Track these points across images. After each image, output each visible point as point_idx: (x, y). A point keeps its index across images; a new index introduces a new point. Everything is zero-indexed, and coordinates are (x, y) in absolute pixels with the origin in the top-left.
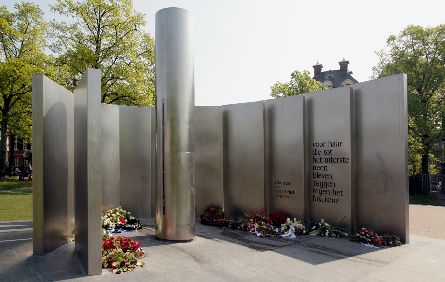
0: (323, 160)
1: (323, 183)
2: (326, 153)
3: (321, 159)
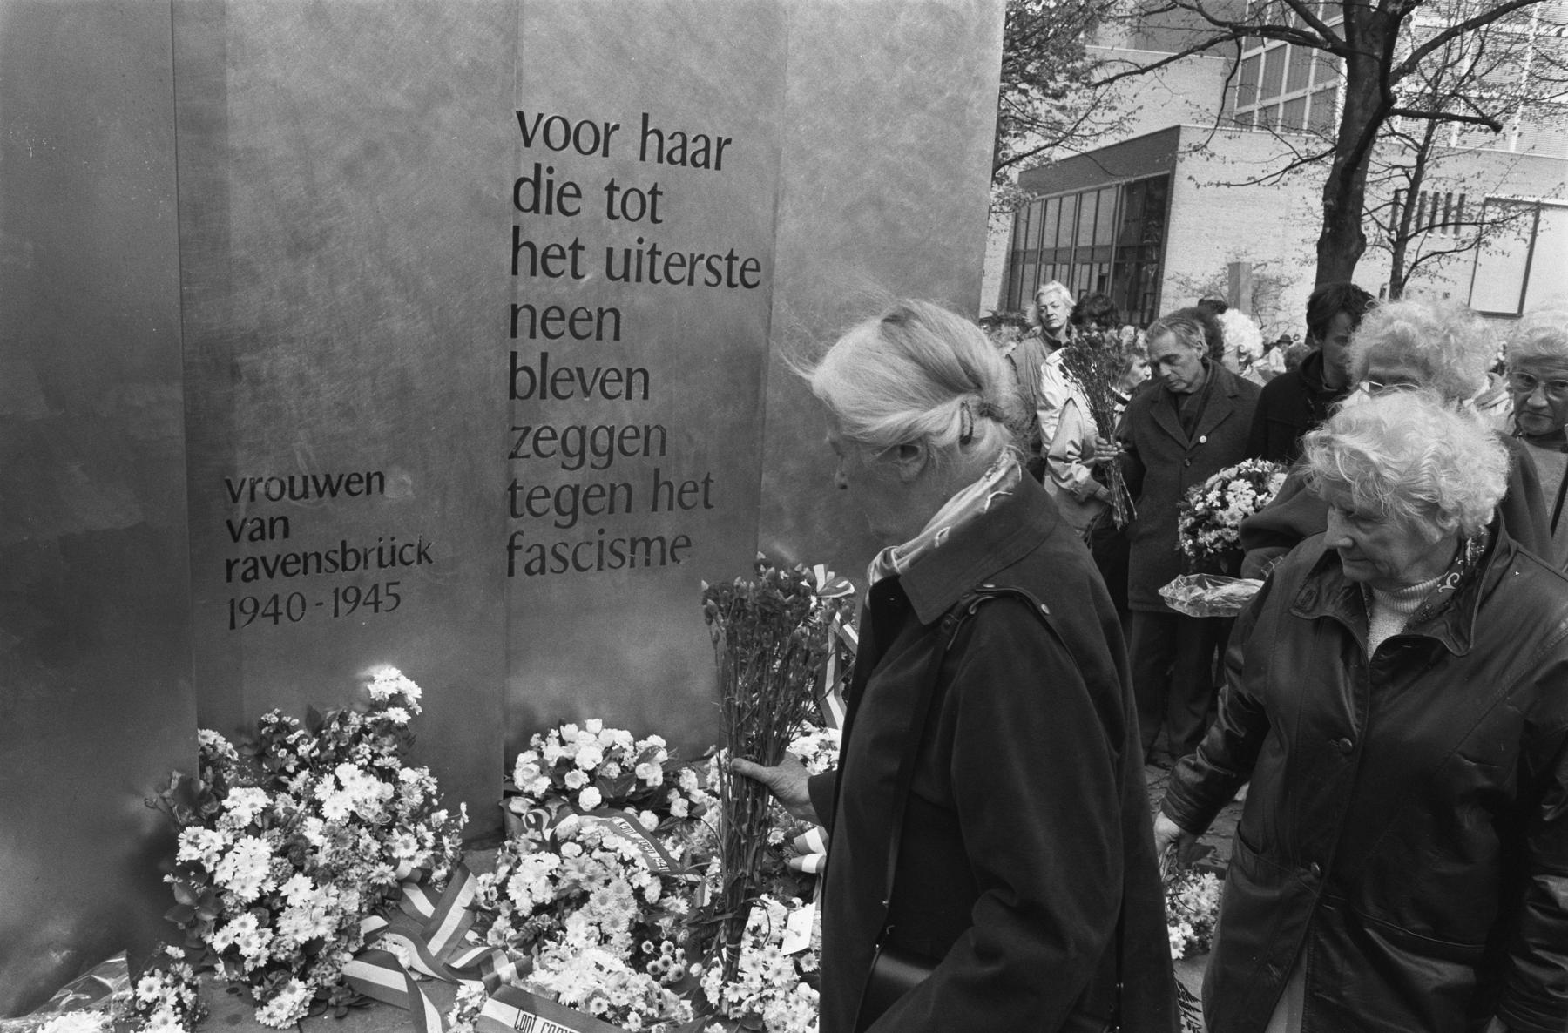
1: (582, 431)
3: (576, 247)
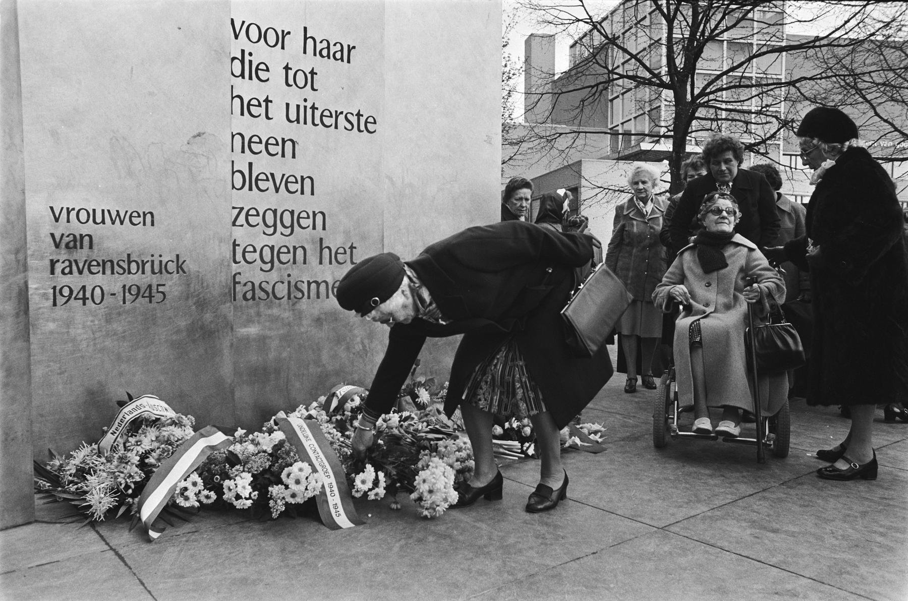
0: (278, 111)
1: (275, 212)
2: (291, 81)
